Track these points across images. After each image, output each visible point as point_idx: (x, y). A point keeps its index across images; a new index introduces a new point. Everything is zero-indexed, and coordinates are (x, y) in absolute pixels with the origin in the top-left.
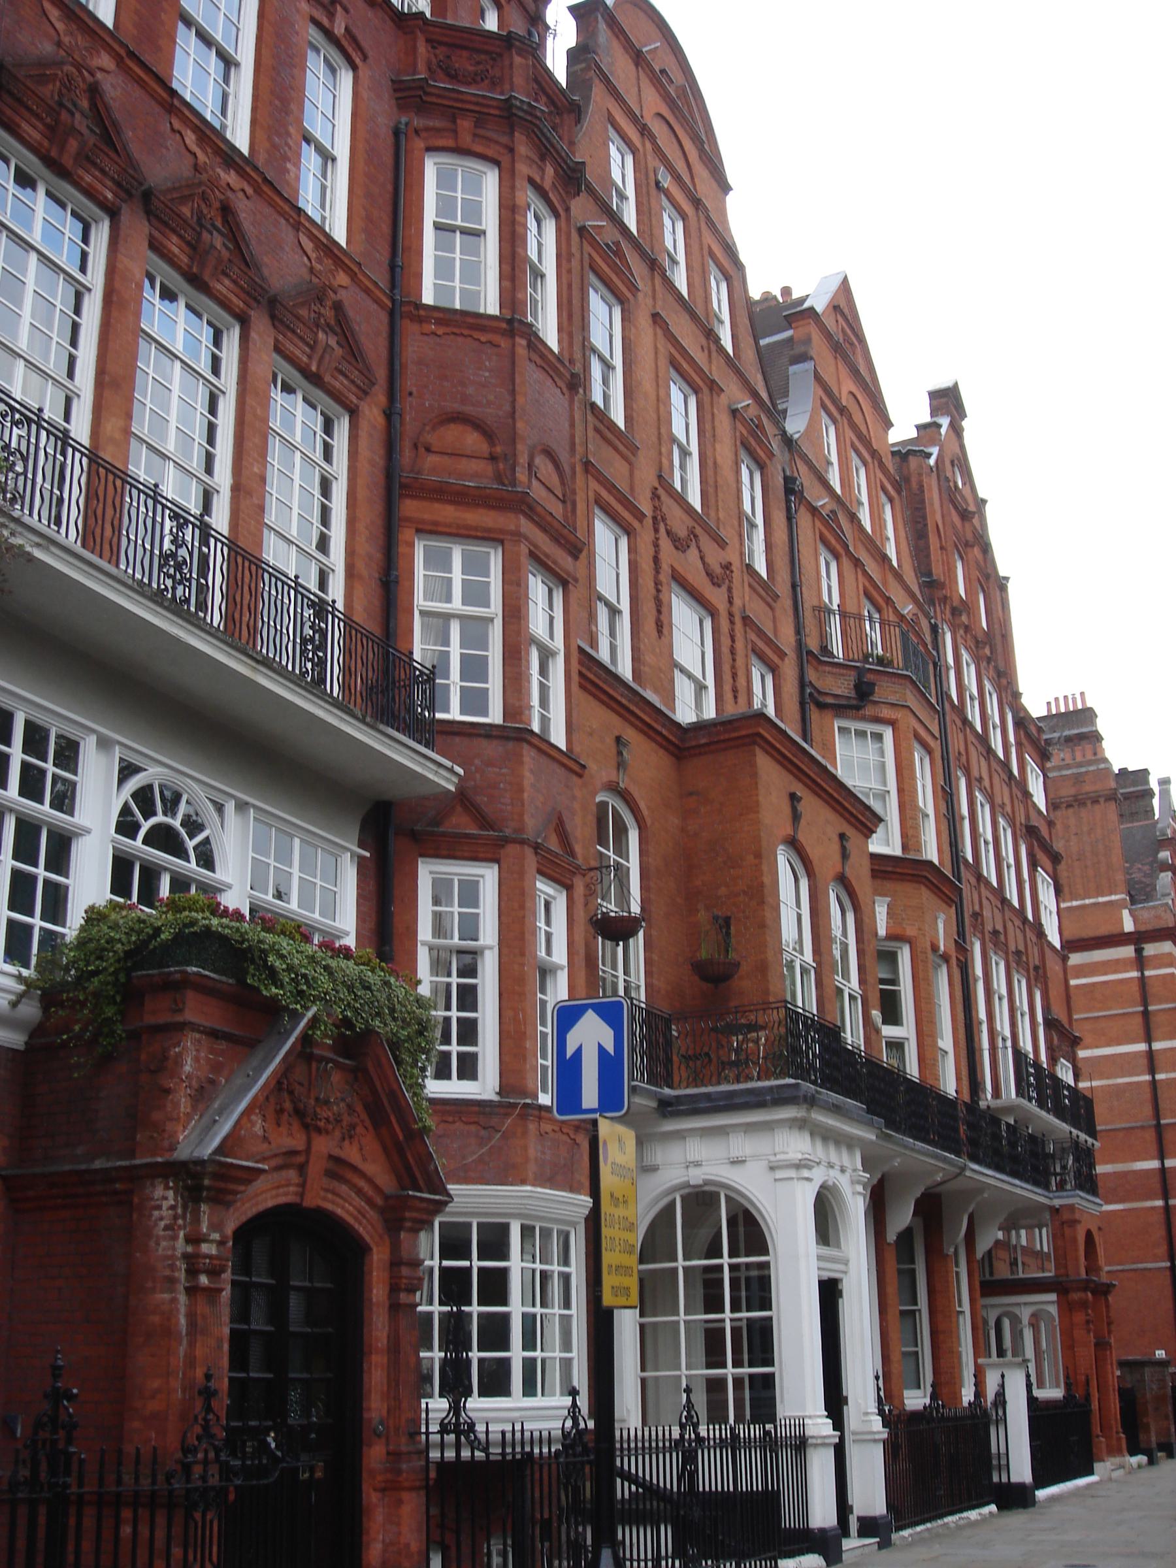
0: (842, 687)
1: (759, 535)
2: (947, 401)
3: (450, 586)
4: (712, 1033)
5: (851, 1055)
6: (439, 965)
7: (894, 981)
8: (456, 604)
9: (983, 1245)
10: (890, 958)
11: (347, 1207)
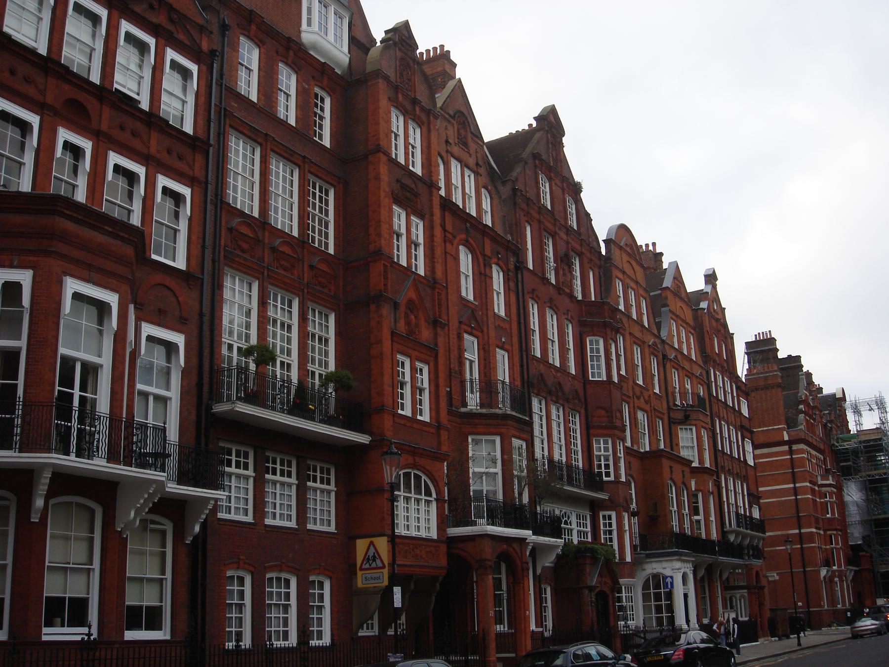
0: (680, 416)
1: (656, 378)
2: (711, 278)
3: (602, 448)
4: (656, 538)
5: (688, 536)
6: (605, 533)
7: (697, 503)
8: (602, 452)
9: (725, 576)
10: (696, 496)
11: (607, 590)
